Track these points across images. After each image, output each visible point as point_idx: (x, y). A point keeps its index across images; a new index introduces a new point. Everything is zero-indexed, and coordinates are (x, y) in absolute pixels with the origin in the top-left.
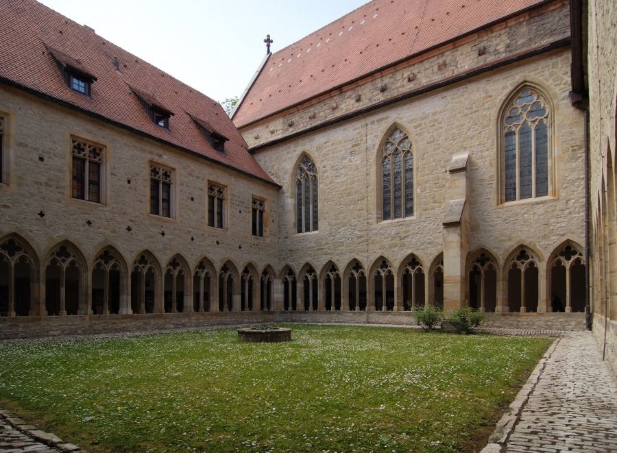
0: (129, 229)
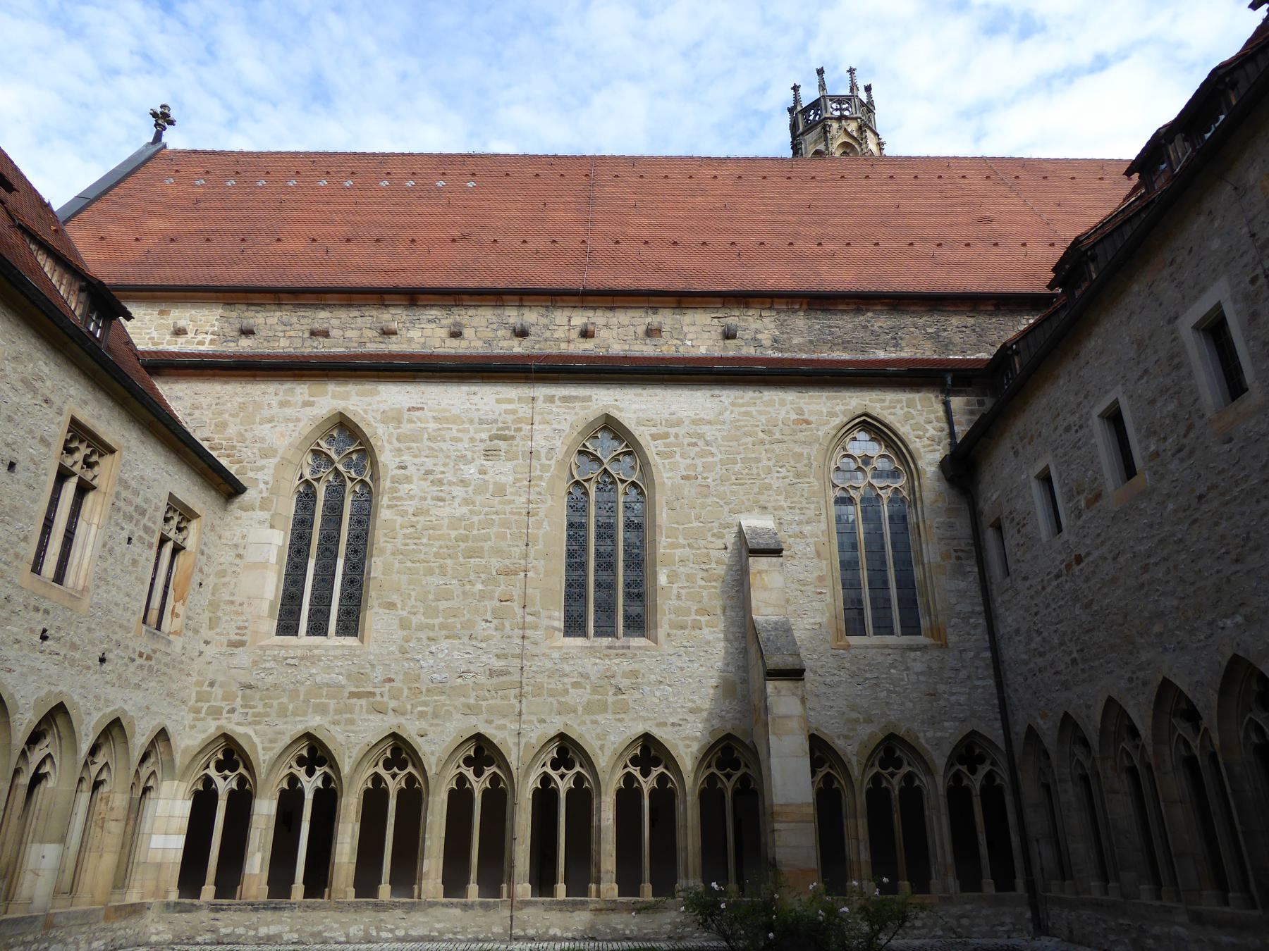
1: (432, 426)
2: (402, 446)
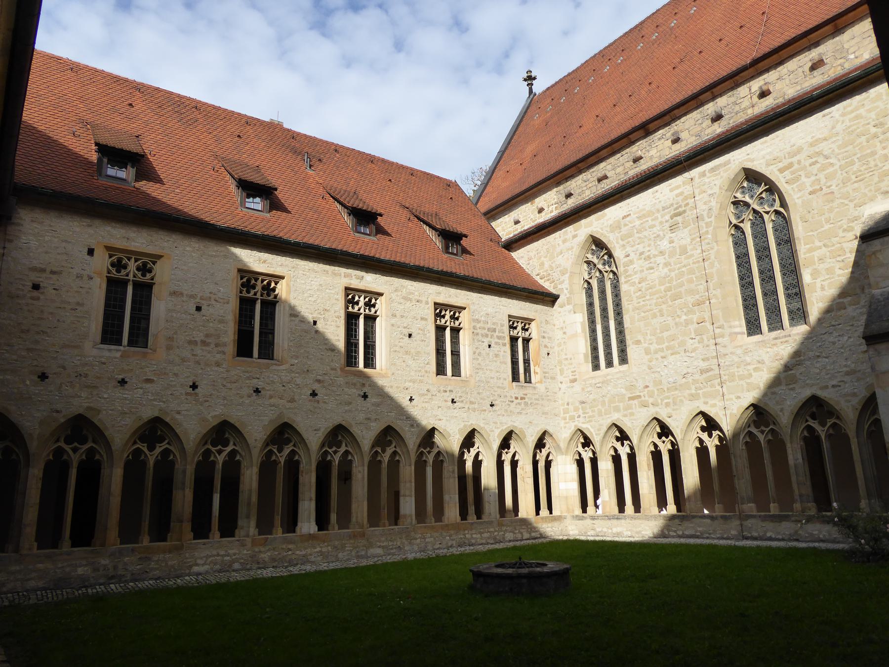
0: (314, 394)
1: (638, 223)
2: (624, 243)
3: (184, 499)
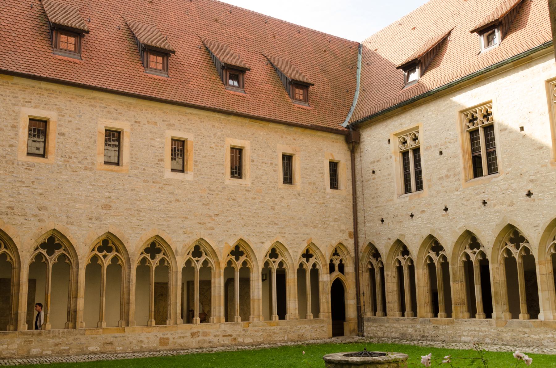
3: (458, 289)
